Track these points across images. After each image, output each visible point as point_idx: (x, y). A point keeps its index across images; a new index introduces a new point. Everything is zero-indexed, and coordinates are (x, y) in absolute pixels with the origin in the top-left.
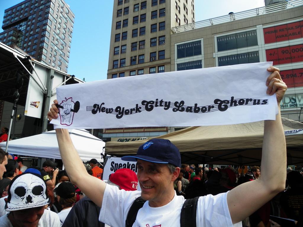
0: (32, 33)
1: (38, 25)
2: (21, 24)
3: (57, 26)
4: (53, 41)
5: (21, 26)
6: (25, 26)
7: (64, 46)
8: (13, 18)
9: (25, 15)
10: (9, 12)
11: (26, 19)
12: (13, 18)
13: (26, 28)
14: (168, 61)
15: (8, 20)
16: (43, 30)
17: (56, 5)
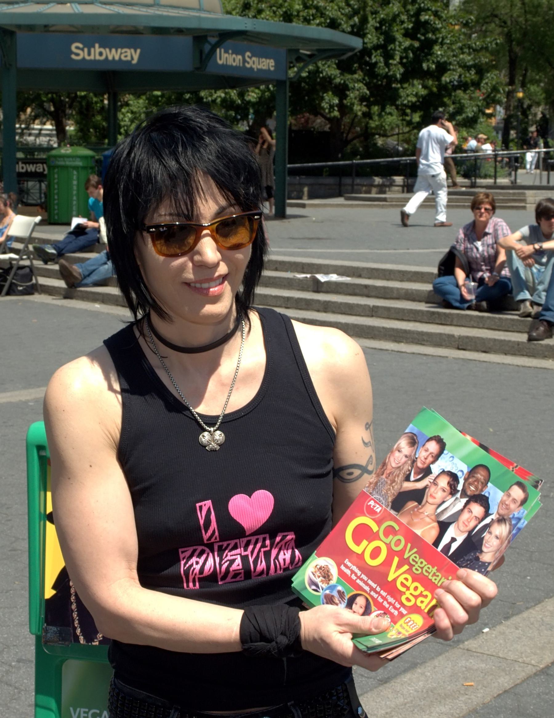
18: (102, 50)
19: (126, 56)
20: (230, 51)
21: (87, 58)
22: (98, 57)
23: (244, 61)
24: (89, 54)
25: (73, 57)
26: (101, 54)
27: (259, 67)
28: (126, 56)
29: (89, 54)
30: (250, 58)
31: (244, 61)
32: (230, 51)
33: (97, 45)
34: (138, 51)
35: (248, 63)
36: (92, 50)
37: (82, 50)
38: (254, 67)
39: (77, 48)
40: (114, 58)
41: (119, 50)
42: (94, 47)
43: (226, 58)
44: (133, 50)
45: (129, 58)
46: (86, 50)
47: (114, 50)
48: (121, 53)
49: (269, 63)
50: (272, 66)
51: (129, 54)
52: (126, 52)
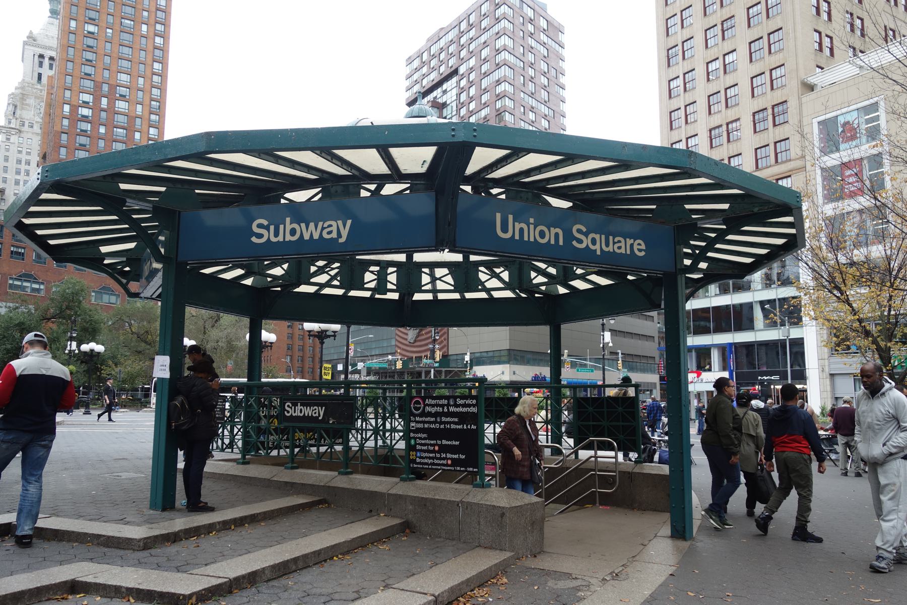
0: (472, 106)
1: (485, 83)
2: (445, 86)
3: (526, 75)
4: (523, 117)
5: (445, 92)
6: (454, 92)
7: (551, 120)
8: (424, 76)
9: (451, 63)
10: (416, 63)
11: (455, 72)
12: (424, 76)
13: (459, 95)
14: (798, 164)
15: (416, 82)
16: (498, 95)
17: (516, 22)
18: (295, 226)
19: (330, 233)
20: (532, 220)
21: (273, 239)
22: (289, 238)
23: (569, 236)
24: (276, 234)
25: (254, 239)
26: (293, 232)
27: (610, 249)
29: (276, 234)
30: (586, 234)
31: (569, 236)
32: (532, 220)
33: (288, 220)
34: (349, 222)
35: (580, 241)
36: (282, 227)
37: (267, 228)
38: (597, 247)
39: (260, 226)
41: (320, 224)
43: (521, 230)
45: (334, 235)
46: (272, 228)
47: (312, 225)
48: (323, 228)
49: (632, 245)
50: (640, 250)
51: (334, 229)
52: (330, 226)
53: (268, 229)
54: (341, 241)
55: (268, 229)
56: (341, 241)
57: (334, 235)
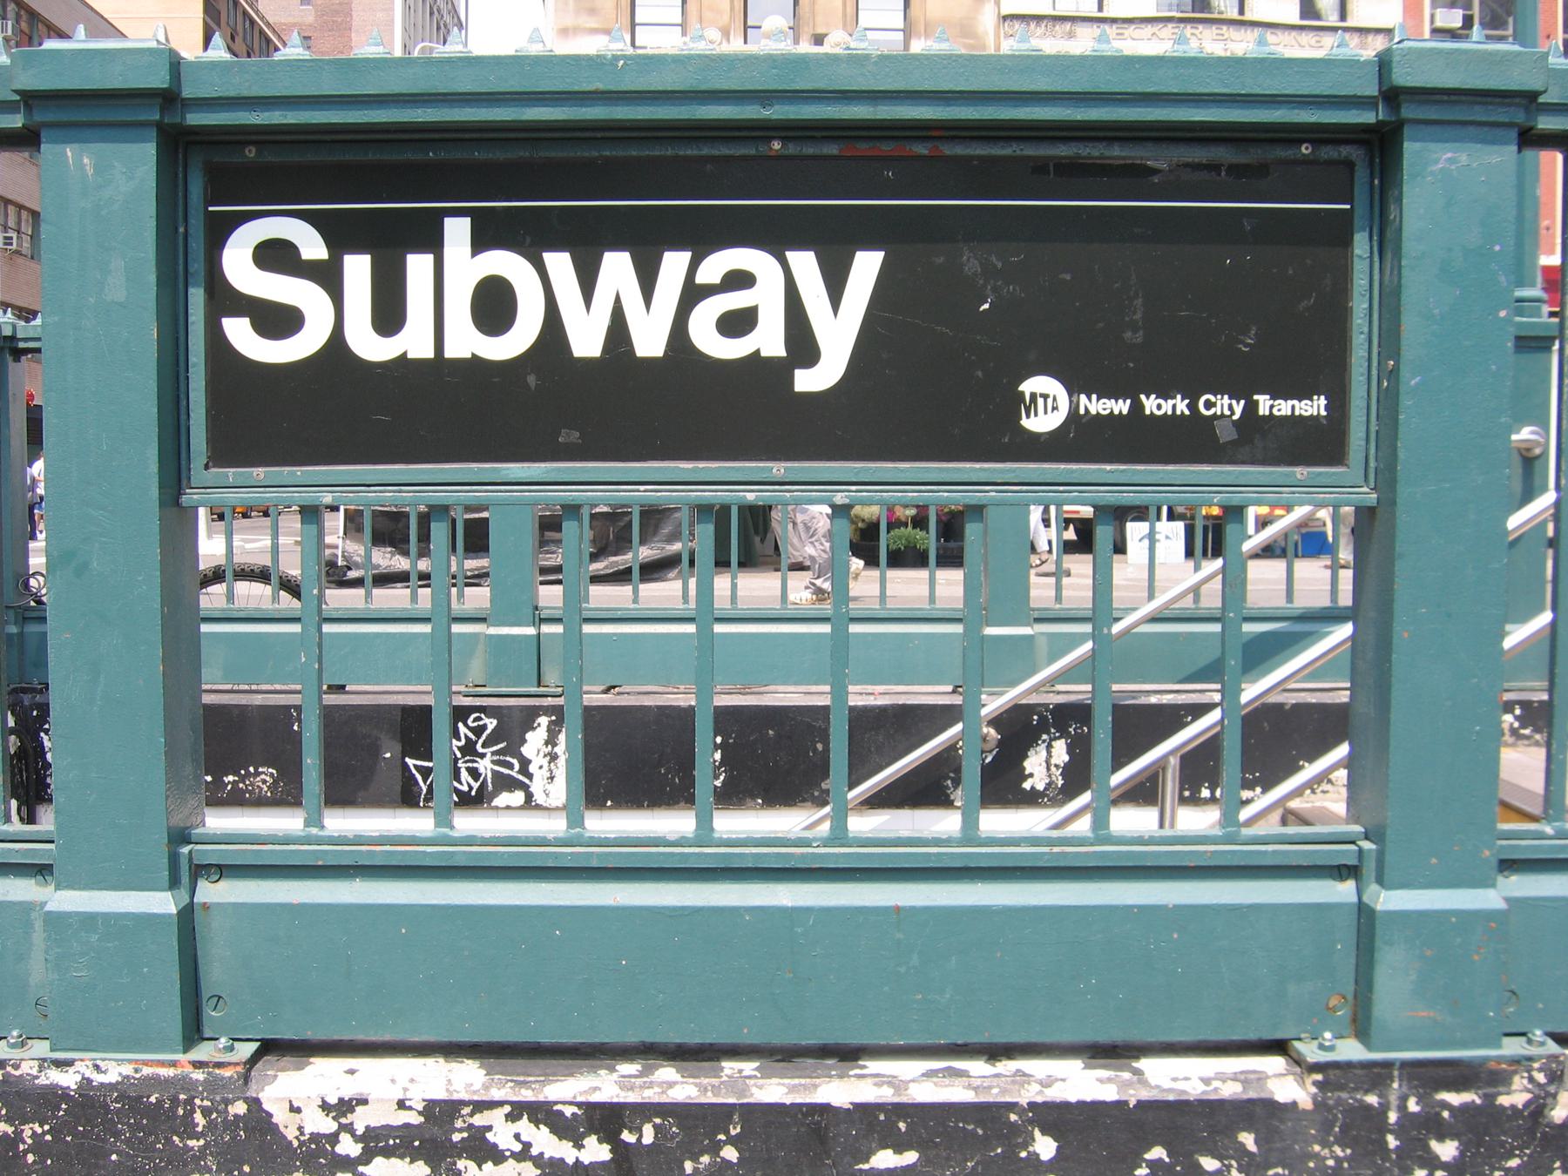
18: (506, 264)
24: (389, 316)
26: (494, 305)
28: (737, 323)
29: (389, 316)
34: (867, 266)
36: (418, 266)
40: (618, 330)
41: (674, 264)
42: (433, 242)
44: (804, 263)
45: (769, 340)
46: (358, 269)
47: (617, 267)
48: (693, 294)
51: (767, 298)
53: (328, 277)
54: (807, 381)
55: (328, 277)
56: (807, 381)
57: (769, 340)
